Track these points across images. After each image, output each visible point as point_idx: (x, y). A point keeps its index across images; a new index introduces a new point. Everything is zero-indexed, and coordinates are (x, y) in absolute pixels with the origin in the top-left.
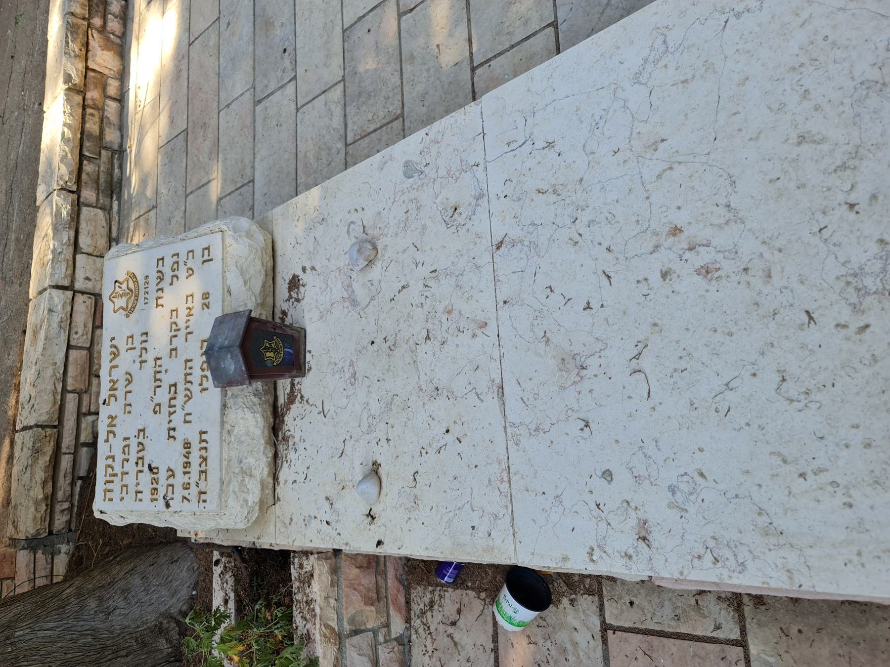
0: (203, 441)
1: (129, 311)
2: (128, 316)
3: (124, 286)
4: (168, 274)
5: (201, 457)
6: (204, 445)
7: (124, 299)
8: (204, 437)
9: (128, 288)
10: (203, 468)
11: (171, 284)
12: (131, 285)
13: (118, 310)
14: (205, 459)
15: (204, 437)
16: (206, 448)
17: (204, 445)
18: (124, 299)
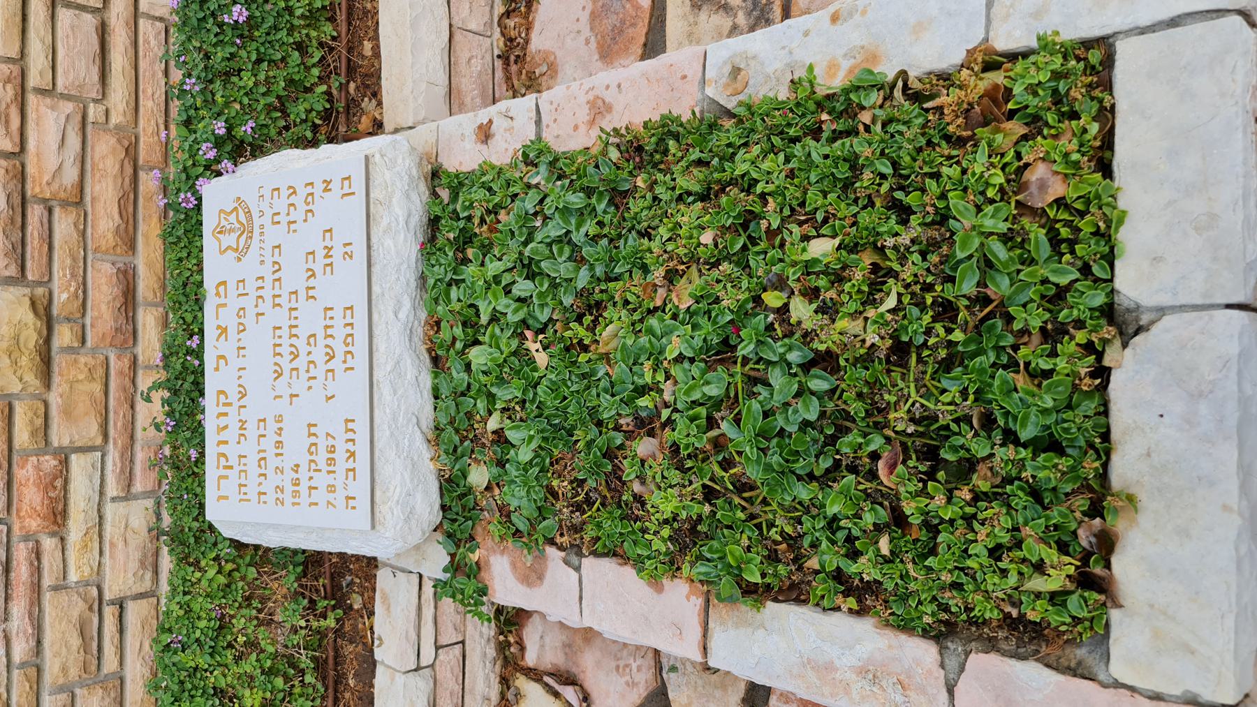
0: (352, 430)
1: (241, 253)
2: (239, 259)
3: (233, 218)
4: (302, 207)
5: (348, 451)
6: (350, 435)
7: (234, 236)
8: (350, 425)
9: (239, 222)
10: (350, 465)
11: (305, 221)
12: (243, 218)
13: (226, 249)
14: (353, 454)
15: (350, 425)
16: (353, 440)
17: (350, 435)
18: (234, 236)
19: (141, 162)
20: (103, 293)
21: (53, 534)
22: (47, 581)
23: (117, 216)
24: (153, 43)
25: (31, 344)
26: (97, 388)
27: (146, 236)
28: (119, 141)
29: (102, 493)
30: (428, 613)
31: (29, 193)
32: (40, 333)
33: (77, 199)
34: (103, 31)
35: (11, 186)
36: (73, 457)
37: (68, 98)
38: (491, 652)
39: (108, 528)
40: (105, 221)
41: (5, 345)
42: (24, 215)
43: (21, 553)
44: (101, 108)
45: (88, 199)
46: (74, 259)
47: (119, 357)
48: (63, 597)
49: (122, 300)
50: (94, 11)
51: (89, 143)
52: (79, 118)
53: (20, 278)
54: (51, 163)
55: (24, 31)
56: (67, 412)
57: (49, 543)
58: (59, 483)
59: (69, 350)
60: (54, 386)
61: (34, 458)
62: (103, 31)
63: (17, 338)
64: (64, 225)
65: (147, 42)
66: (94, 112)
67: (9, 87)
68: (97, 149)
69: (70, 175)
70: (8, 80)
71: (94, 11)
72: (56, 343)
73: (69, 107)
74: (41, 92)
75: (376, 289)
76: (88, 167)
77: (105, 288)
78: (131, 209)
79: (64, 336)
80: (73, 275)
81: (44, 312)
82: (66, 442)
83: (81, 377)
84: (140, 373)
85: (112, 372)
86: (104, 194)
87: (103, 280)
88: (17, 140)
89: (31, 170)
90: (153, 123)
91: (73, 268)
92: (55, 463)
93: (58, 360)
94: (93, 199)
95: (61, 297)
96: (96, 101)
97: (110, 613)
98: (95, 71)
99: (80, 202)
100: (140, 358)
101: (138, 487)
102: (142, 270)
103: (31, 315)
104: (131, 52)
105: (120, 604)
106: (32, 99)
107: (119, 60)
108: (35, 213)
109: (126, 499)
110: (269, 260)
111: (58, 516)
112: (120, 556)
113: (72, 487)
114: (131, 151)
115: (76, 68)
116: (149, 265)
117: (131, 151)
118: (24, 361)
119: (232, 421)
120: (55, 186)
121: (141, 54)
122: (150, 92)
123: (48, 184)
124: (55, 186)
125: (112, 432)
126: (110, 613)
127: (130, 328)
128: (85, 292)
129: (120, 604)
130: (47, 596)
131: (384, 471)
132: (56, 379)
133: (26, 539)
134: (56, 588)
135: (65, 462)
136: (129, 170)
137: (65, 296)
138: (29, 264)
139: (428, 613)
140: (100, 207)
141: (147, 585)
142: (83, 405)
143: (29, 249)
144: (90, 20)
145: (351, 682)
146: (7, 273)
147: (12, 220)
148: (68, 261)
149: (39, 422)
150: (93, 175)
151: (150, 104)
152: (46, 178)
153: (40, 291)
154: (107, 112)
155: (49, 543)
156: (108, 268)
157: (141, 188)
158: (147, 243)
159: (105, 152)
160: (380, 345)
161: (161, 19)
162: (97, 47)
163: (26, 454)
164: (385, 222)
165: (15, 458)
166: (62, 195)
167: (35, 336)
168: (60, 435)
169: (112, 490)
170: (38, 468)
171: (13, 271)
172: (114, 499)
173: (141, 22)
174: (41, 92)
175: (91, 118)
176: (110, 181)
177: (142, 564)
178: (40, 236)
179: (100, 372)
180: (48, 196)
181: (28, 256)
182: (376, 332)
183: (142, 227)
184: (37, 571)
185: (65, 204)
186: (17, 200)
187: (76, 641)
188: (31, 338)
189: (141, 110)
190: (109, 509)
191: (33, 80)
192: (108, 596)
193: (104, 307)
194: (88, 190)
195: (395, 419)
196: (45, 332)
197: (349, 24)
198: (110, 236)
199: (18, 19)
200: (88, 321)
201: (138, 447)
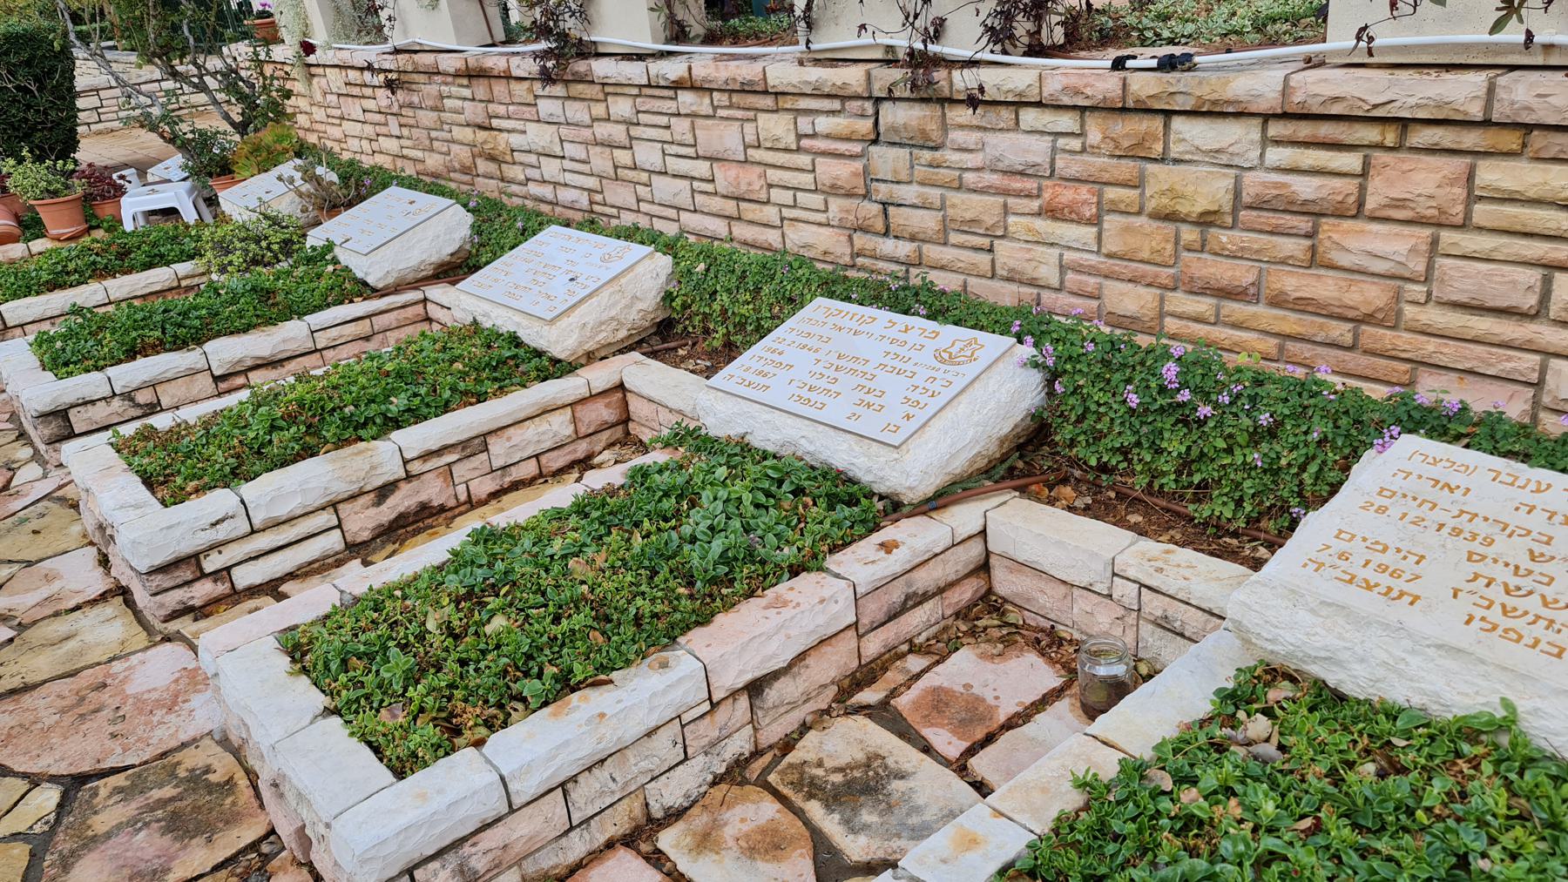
19: (1364, 327)
21: (1040, 207)
22: (1011, 201)
24: (1509, 365)
25: (1178, 207)
26: (1145, 255)
27: (1284, 318)
28: (1380, 309)
29: (1069, 248)
33: (1315, 260)
36: (1095, 230)
37: (1430, 267)
39: (1041, 249)
40: (1293, 283)
41: (1177, 187)
42: (1304, 213)
43: (1030, 185)
45: (1322, 272)
46: (1257, 251)
48: (998, 210)
51: (1382, 281)
54: (1352, 243)
56: (1127, 229)
57: (1035, 205)
58: (1074, 216)
60: (1151, 222)
61: (1095, 200)
63: (1183, 197)
64: (1293, 247)
65: (1509, 359)
67: (1436, 212)
68: (1374, 287)
69: (1344, 260)
72: (1184, 228)
73: (1418, 265)
74: (1435, 242)
76: (1357, 277)
77: (1230, 273)
78: (1310, 309)
80: (1243, 249)
81: (1206, 220)
82: (1106, 226)
86: (1324, 287)
87: (1238, 273)
90: (1407, 347)
91: (1250, 249)
92: (1088, 214)
93: (1170, 228)
94: (1319, 276)
95: (1224, 237)
96: (1429, 294)
97: (986, 242)
98: (1463, 298)
101: (1070, 276)
102: (1252, 309)
103: (1200, 210)
104: (1496, 340)
105: (991, 250)
106: (1427, 232)
108: (1304, 224)
109: (1061, 266)
111: (1052, 212)
112: (1020, 255)
113: (1074, 226)
114: (1368, 319)
115: (1461, 279)
116: (1254, 315)
118: (1165, 201)
119: (846, 323)
121: (1494, 350)
122: (1445, 350)
125: (1112, 261)
126: (986, 242)
129: (991, 250)
130: (1001, 200)
132: (1156, 224)
133: (1040, 189)
134: (1005, 205)
135: (1089, 222)
136: (1351, 314)
137: (1224, 239)
138: (1254, 213)
140: (1312, 281)
141: (999, 272)
142: (1133, 241)
143: (1271, 214)
144: (1531, 301)
147: (1292, 203)
149: (1122, 207)
151: (1431, 348)
152: (1335, 237)
155: (1035, 205)
157: (1334, 323)
158: (1276, 318)
159: (1371, 295)
160: (791, 420)
163: (1100, 195)
164: (857, 449)
165: (1097, 187)
166: (1321, 249)
168: (1111, 222)
169: (1069, 256)
170: (1085, 202)
172: (1061, 255)
173: (1537, 358)
174: (1435, 242)
176: (1336, 294)
177: (1011, 270)
178: (1277, 226)
179: (1159, 260)
182: (798, 420)
184: (1018, 194)
185: (1313, 249)
187: (968, 216)
189: (1425, 338)
190: (1056, 252)
191: (1447, 236)
192: (996, 242)
193: (1212, 270)
194: (1331, 273)
195: (753, 417)
197: (1168, 511)
199: (1519, 228)
200: (1204, 256)
201: (1099, 280)
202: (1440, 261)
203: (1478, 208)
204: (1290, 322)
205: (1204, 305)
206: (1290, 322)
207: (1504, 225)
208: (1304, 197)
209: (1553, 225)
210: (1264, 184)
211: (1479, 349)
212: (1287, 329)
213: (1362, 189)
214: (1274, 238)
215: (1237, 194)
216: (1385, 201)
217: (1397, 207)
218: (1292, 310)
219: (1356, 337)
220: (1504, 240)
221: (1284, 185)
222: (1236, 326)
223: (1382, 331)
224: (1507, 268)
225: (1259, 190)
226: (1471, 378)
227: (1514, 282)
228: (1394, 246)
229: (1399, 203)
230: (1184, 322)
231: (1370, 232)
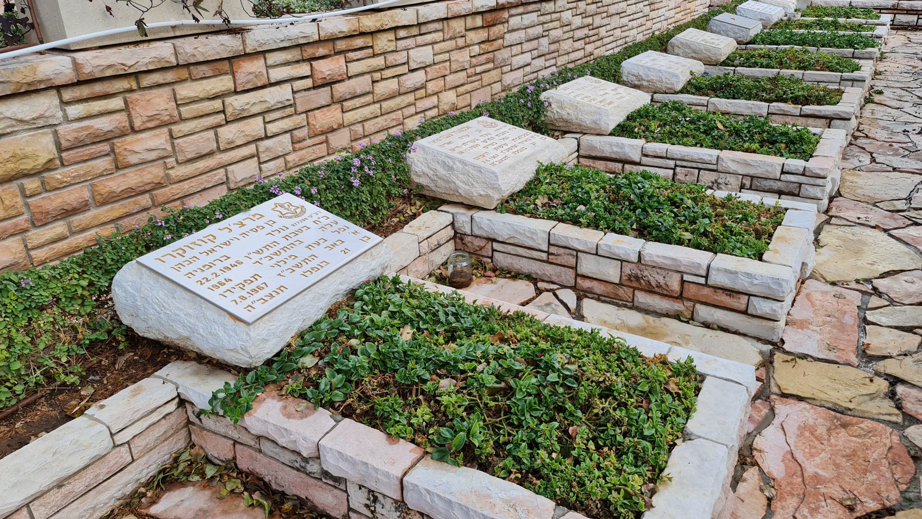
20: (71, 196)
23: (120, 189)
24: (216, 178)
27: (112, 209)
30: (155, 417)
31: (115, 141)
32: (32, 169)
33: (119, 166)
34: (210, 154)
35: (117, 131)
38: (129, 489)
41: (19, 152)
42: (99, 142)
44: (175, 164)
45: (122, 172)
46: (84, 175)
47: (26, 220)
49: (70, 208)
50: (218, 148)
52: (166, 154)
53: (60, 149)
54: (137, 148)
55: (195, 118)
59: (22, 190)
62: (210, 154)
63: (26, 157)
64: (103, 164)
65: (215, 175)
66: (171, 161)
69: (133, 159)
70: (171, 116)
71: (218, 148)
73: (170, 148)
74: (170, 132)
75: (344, 269)
76: (140, 167)
79: (31, 184)
80: (74, 177)
81: (48, 167)
83: (7, 202)
84: (18, 237)
85: (14, 220)
86: (131, 179)
88: (142, 128)
89: (129, 139)
91: (79, 176)
95: (58, 175)
99: (117, 168)
100: (29, 234)
102: (89, 214)
103: (44, 161)
104: (207, 170)
106: (165, 130)
107: (201, 165)
108: (105, 147)
110: (296, 228)
114: (159, 185)
115: (189, 146)
116: (95, 217)
117: (159, 185)
118: (10, 166)
120: (125, 153)
123: (125, 149)
124: (125, 153)
127: (50, 220)
128: (64, 187)
131: (277, 315)
136: (148, 188)
137: (59, 177)
138: (71, 152)
139: (155, 417)
140: (121, 179)
145: (18, 425)
146: (63, 142)
148: (82, 172)
150: (137, 171)
151: (187, 187)
152: (128, 147)
153: (58, 162)
154: (173, 168)
156: (87, 195)
157: (140, 197)
158: (107, 211)
159: (154, 173)
161: (227, 178)
162: (204, 153)
166: (120, 158)
167: (29, 167)
171: (64, 144)
173: (222, 170)
174: (170, 132)
175: (167, 161)
176: (140, 180)
178: (92, 153)
179: (14, 213)
180: (117, 151)
181: (76, 150)
182: (329, 278)
183: (117, 205)
185: (116, 160)
186: (109, 136)
188: (28, 165)
191: (174, 128)
193: (60, 200)
194: (127, 171)
196: (32, 172)
198: (107, 190)
199: (201, 114)
200: (44, 195)
202: (176, 142)
203: (182, 109)
204: (117, 209)
205: (59, 228)
206: (117, 209)
207: (195, 114)
208: (106, 130)
209: (211, 108)
210: (74, 131)
211: (203, 176)
212: (117, 214)
213: (129, 116)
214: (88, 163)
215: (58, 145)
216: (145, 119)
217: (150, 121)
218: (113, 202)
219: (153, 200)
220: (196, 122)
221: (87, 128)
222: (83, 230)
223: (163, 190)
224: (202, 134)
225: (75, 135)
226: (206, 192)
227: (208, 139)
228: (157, 140)
229: (151, 118)
230: (46, 249)
231: (142, 139)
